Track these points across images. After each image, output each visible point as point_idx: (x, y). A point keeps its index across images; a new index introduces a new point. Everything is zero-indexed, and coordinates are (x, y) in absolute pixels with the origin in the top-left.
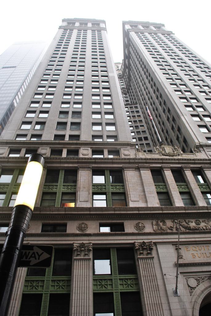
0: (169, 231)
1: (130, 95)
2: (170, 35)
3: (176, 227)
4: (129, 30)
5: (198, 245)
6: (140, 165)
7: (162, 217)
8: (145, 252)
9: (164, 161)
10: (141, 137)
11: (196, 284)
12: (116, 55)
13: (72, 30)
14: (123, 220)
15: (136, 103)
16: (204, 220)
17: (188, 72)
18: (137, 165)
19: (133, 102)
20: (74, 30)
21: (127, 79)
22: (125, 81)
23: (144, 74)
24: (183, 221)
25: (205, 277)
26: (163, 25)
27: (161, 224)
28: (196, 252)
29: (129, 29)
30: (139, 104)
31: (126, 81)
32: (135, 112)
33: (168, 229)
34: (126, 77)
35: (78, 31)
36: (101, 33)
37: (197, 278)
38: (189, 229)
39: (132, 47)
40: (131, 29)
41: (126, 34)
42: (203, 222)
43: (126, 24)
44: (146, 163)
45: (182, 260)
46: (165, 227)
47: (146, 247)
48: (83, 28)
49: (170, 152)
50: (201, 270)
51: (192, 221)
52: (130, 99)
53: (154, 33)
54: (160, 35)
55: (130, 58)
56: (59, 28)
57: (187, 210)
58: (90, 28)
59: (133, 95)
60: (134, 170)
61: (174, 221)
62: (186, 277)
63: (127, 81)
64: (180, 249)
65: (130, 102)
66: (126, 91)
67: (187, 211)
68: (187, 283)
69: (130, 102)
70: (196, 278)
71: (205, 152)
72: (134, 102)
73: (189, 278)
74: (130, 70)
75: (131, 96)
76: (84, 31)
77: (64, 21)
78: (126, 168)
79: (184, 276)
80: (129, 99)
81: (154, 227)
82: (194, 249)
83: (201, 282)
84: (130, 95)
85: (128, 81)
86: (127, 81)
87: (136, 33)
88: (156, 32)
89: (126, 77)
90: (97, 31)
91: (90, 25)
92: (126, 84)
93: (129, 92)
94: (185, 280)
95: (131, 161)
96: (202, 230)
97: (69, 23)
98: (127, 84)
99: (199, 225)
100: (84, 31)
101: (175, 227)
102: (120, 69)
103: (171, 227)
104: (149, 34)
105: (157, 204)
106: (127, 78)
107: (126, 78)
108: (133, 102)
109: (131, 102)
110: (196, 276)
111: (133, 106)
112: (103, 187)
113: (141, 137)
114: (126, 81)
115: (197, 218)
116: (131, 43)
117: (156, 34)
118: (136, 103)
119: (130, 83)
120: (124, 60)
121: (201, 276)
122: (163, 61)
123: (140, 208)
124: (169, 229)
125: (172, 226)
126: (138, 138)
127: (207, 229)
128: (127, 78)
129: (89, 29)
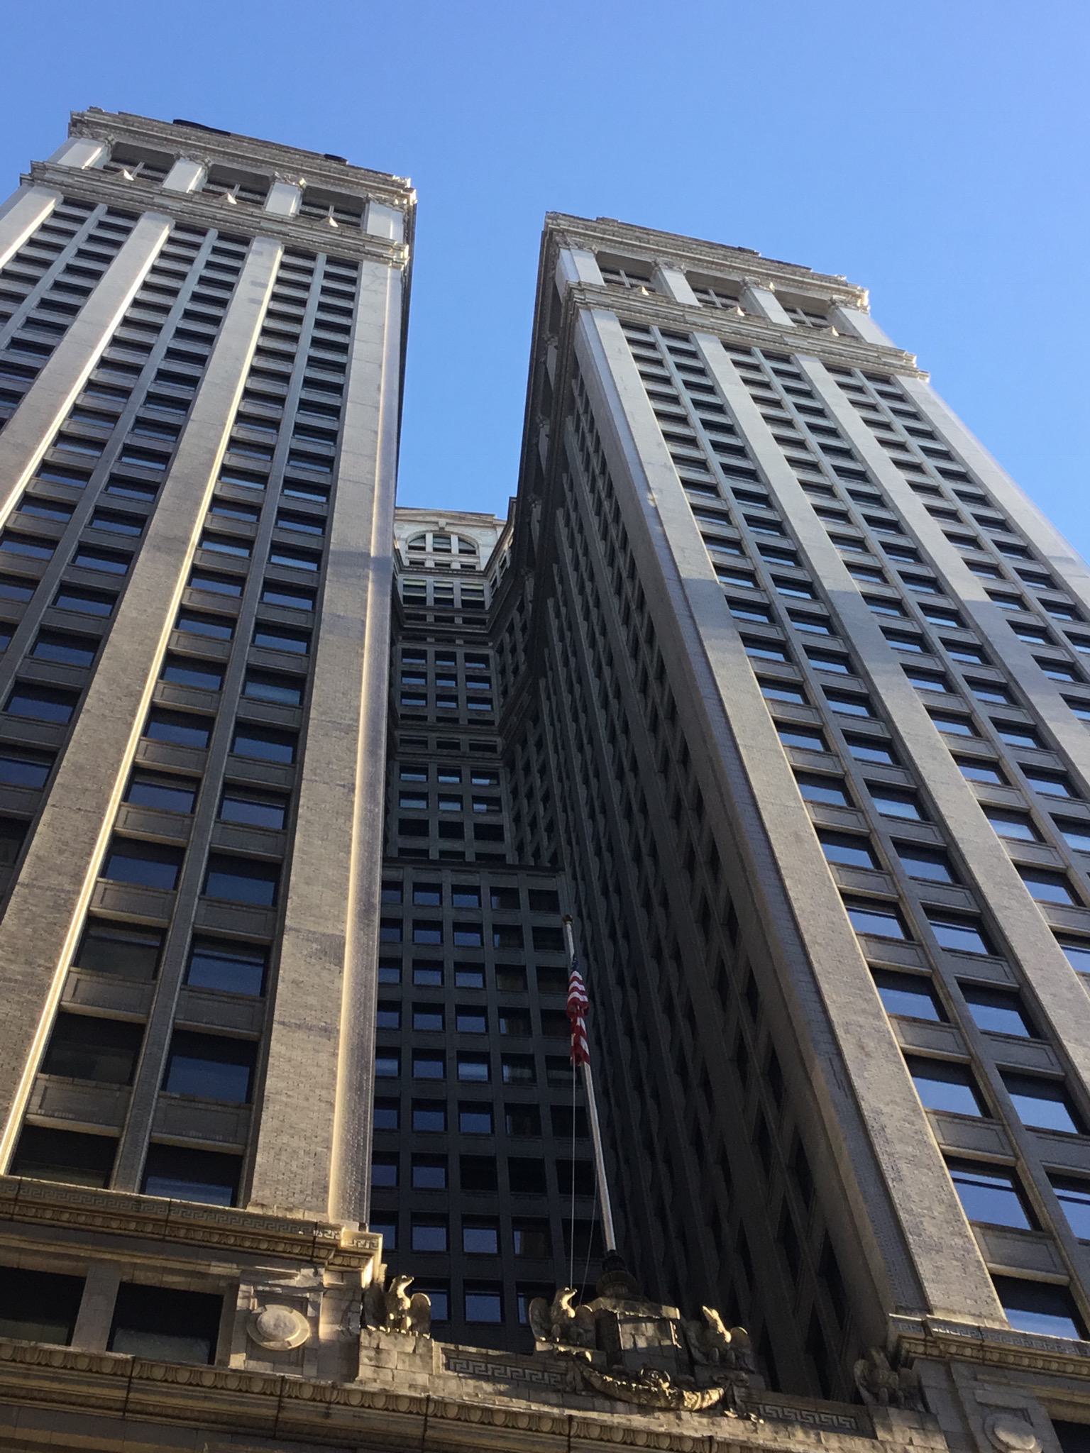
1: (523, 790)
2: (886, 380)
4: (577, 296)
10: (541, 1162)
12: (433, 470)
13: (124, 217)
15: (555, 866)
17: (963, 697)
19: (529, 850)
20: (143, 224)
21: (522, 657)
22: (503, 672)
23: (627, 652)
29: (582, 288)
30: (575, 878)
31: (510, 669)
32: (528, 937)
34: (518, 634)
36: (353, 281)
39: (584, 424)
40: (599, 291)
41: (556, 314)
48: (221, 214)
52: (517, 819)
53: (770, 346)
54: (813, 369)
55: (563, 504)
58: (275, 229)
59: (539, 795)
63: (516, 671)
65: (506, 848)
66: (492, 749)
69: (506, 848)
72: (537, 854)
74: (545, 588)
75: (530, 795)
80: (505, 819)
84: (523, 790)
85: (523, 668)
86: (516, 671)
87: (625, 325)
88: (789, 340)
89: (518, 634)
90: (330, 261)
91: (284, 202)
92: (505, 693)
93: (520, 764)
97: (121, 156)
98: (512, 692)
102: (482, 566)
104: (728, 347)
106: (520, 647)
107: (513, 650)
108: (529, 850)
109: (520, 848)
111: (524, 884)
113: (541, 1162)
114: (510, 669)
116: (576, 393)
117: (786, 359)
118: (554, 858)
119: (535, 694)
120: (520, 507)
122: (779, 581)
126: (512, 1161)
128: (520, 647)
129: (270, 234)
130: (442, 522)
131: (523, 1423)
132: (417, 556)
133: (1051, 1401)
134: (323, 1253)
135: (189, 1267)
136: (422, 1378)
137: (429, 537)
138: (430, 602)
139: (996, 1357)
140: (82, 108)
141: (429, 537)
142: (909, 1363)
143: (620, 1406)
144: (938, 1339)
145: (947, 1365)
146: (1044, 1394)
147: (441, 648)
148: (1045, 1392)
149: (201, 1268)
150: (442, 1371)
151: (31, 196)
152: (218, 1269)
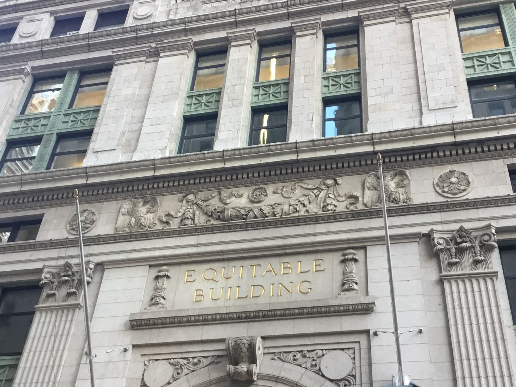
0: (159, 227)
3: (184, 214)
5: (226, 264)
6: (165, 41)
7: (153, 188)
8: (63, 292)
9: (241, 18)
11: (168, 378)
14: (41, 207)
16: (280, 185)
18: (153, 45)
24: (216, 193)
25: (204, 357)
27: (142, 210)
28: (212, 284)
33: (156, 222)
37: (180, 360)
38: (219, 218)
42: (274, 193)
44: (186, 31)
45: (154, 308)
46: (150, 216)
47: (67, 278)
50: (199, 338)
51: (241, 192)
57: (230, 160)
60: (145, 58)
61: (184, 197)
62: (146, 358)
64: (168, 277)
67: (228, 165)
68: (143, 375)
70: (172, 361)
73: (156, 360)
78: (120, 57)
79: (141, 355)
81: (121, 218)
82: (210, 275)
83: (186, 371)
94: (141, 367)
95: (141, 34)
96: (256, 217)
99: (259, 202)
101: (180, 214)
103: (168, 215)
105: (159, 151)
110: (180, 356)
112: (43, 122)
115: (257, 183)
121: (193, 355)
123: (93, 169)
124: (162, 222)
125: (173, 213)
127: (274, 212)
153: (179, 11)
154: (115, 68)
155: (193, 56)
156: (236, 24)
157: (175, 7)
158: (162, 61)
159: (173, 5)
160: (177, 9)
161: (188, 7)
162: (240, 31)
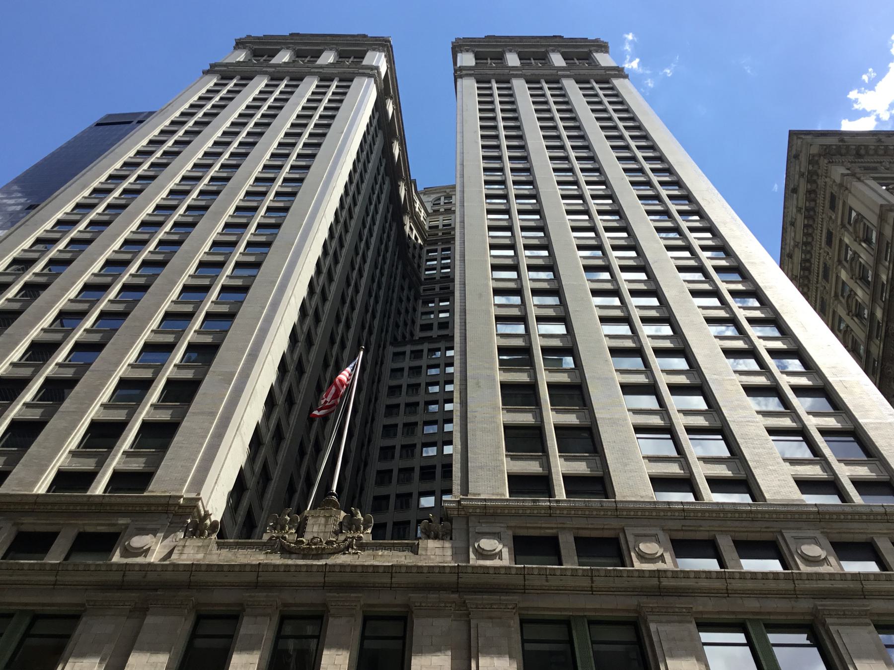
26: (603, 47)
35: (321, 80)
43: (461, 52)
49: (321, 536)
56: (203, 73)
71: (468, 534)
76: (340, 80)
77: (240, 44)
97: (256, 54)
100: (340, 80)
130: (448, 191)
131: (293, 569)
132: (436, 208)
133: (515, 527)
134: (172, 508)
135: (107, 522)
136: (200, 556)
137: (442, 198)
138: (441, 227)
139: (491, 511)
140: (242, 35)
141: (442, 198)
142: (450, 520)
143: (294, 556)
144: (465, 507)
145: (468, 518)
146: (513, 524)
147: (443, 246)
148: (513, 523)
149: (113, 522)
150: (219, 552)
151: (207, 77)
152: (122, 521)
153: (186, 550)
154: (84, 619)
155: (192, 618)
156: (256, 586)
157: (181, 543)
158: (150, 620)
159: (181, 539)
160: (184, 546)
161: (199, 547)
162: (261, 596)
